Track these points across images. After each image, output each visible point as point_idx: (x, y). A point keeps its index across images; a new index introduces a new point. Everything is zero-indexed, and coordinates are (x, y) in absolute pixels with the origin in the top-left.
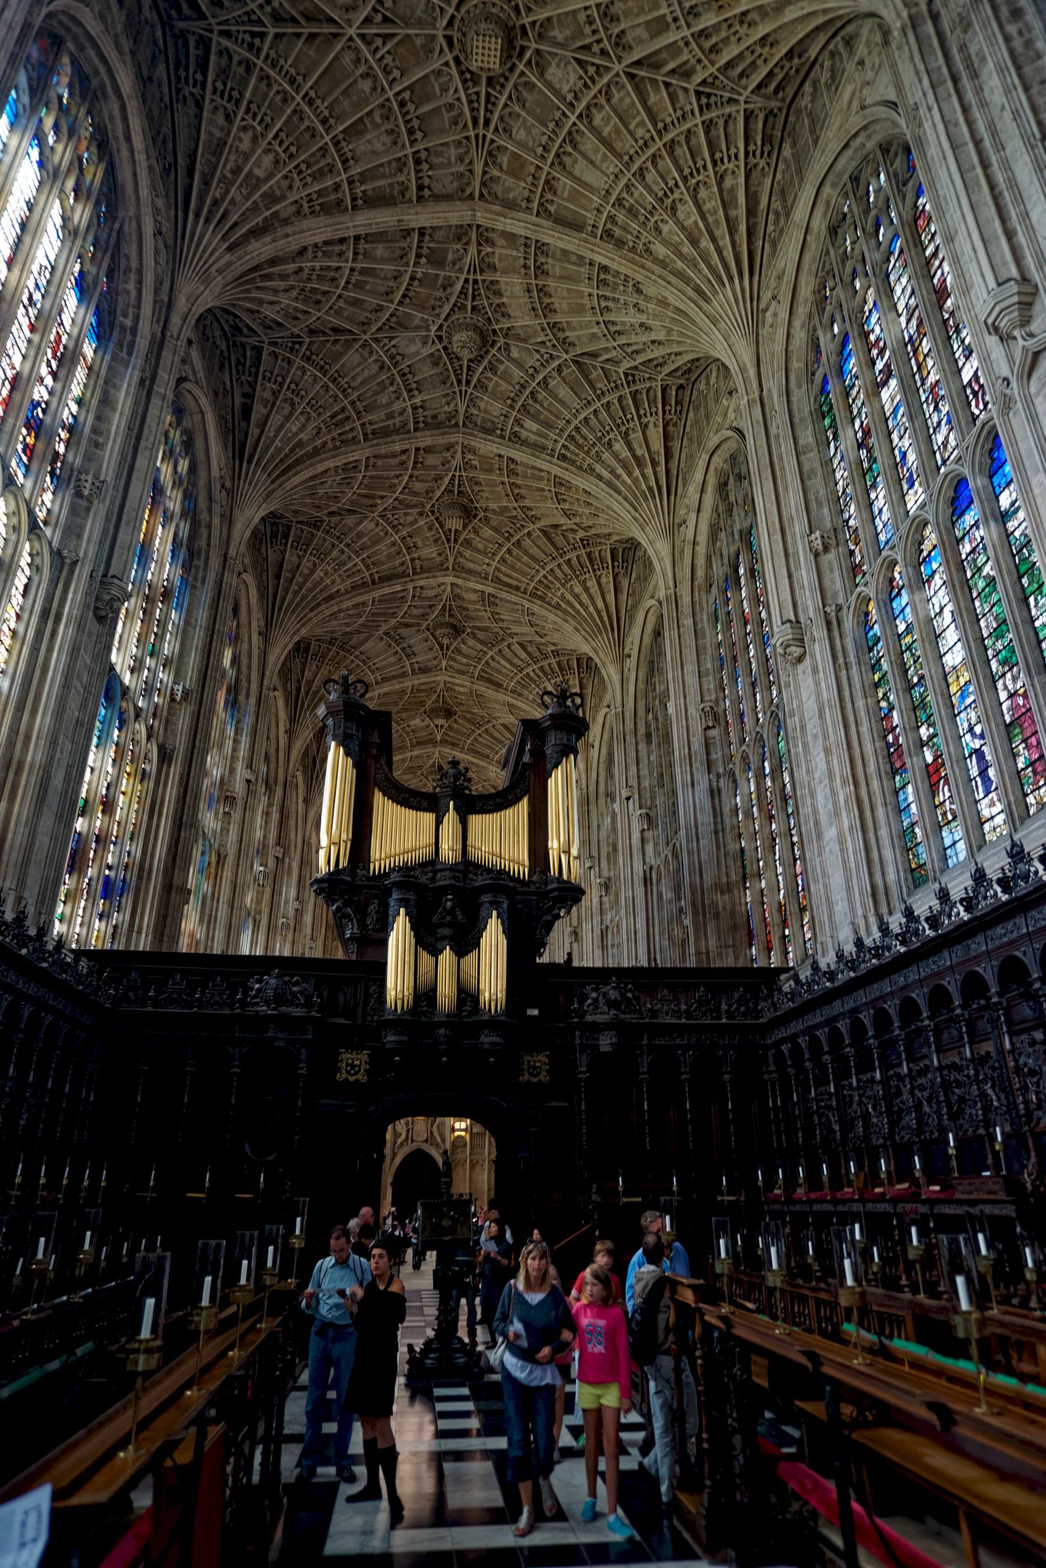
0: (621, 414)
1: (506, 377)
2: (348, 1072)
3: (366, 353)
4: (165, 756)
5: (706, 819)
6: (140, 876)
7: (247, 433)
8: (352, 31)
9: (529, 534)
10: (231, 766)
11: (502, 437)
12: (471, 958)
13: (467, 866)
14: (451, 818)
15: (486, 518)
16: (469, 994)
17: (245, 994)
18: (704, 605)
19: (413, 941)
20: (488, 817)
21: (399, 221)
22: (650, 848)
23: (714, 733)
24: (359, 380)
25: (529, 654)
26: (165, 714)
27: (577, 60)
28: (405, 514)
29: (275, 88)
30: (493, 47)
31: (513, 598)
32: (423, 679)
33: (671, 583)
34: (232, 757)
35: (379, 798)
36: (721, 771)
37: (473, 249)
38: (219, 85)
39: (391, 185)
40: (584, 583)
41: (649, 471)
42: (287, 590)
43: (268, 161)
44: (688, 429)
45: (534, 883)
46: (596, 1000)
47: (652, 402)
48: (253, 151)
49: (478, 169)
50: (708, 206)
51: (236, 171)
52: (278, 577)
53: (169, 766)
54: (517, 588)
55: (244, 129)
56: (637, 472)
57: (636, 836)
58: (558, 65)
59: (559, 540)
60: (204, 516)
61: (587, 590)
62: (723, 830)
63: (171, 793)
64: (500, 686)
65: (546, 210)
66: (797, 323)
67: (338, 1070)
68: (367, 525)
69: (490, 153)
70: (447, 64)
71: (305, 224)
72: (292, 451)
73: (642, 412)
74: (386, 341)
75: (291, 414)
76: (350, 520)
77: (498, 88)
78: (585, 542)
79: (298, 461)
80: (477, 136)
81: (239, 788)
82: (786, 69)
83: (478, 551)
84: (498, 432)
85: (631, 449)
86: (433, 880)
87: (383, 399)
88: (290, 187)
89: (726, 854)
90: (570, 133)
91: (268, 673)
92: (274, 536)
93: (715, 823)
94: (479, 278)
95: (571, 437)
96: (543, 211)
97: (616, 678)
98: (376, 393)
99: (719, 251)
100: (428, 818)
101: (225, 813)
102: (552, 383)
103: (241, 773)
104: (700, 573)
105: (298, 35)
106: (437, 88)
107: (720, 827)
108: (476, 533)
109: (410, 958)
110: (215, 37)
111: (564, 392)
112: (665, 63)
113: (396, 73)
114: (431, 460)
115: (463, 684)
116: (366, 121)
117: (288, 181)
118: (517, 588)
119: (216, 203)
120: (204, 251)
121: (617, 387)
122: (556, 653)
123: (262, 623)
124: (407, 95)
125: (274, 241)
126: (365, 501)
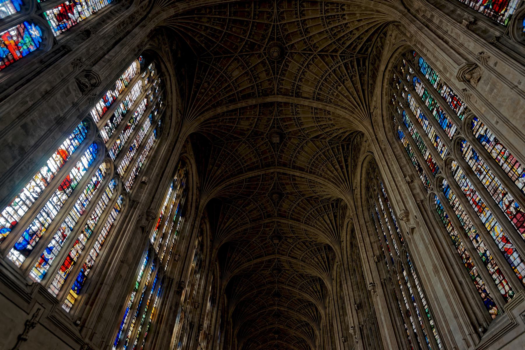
1: (285, 275)
40: (308, 310)
51: (233, 261)
66: (338, 286)
68: (257, 299)
83: (282, 301)
96: (289, 256)
97: (318, 334)
99: (323, 266)
104: (331, 321)
111: (297, 278)
115: (281, 327)
122: (305, 321)
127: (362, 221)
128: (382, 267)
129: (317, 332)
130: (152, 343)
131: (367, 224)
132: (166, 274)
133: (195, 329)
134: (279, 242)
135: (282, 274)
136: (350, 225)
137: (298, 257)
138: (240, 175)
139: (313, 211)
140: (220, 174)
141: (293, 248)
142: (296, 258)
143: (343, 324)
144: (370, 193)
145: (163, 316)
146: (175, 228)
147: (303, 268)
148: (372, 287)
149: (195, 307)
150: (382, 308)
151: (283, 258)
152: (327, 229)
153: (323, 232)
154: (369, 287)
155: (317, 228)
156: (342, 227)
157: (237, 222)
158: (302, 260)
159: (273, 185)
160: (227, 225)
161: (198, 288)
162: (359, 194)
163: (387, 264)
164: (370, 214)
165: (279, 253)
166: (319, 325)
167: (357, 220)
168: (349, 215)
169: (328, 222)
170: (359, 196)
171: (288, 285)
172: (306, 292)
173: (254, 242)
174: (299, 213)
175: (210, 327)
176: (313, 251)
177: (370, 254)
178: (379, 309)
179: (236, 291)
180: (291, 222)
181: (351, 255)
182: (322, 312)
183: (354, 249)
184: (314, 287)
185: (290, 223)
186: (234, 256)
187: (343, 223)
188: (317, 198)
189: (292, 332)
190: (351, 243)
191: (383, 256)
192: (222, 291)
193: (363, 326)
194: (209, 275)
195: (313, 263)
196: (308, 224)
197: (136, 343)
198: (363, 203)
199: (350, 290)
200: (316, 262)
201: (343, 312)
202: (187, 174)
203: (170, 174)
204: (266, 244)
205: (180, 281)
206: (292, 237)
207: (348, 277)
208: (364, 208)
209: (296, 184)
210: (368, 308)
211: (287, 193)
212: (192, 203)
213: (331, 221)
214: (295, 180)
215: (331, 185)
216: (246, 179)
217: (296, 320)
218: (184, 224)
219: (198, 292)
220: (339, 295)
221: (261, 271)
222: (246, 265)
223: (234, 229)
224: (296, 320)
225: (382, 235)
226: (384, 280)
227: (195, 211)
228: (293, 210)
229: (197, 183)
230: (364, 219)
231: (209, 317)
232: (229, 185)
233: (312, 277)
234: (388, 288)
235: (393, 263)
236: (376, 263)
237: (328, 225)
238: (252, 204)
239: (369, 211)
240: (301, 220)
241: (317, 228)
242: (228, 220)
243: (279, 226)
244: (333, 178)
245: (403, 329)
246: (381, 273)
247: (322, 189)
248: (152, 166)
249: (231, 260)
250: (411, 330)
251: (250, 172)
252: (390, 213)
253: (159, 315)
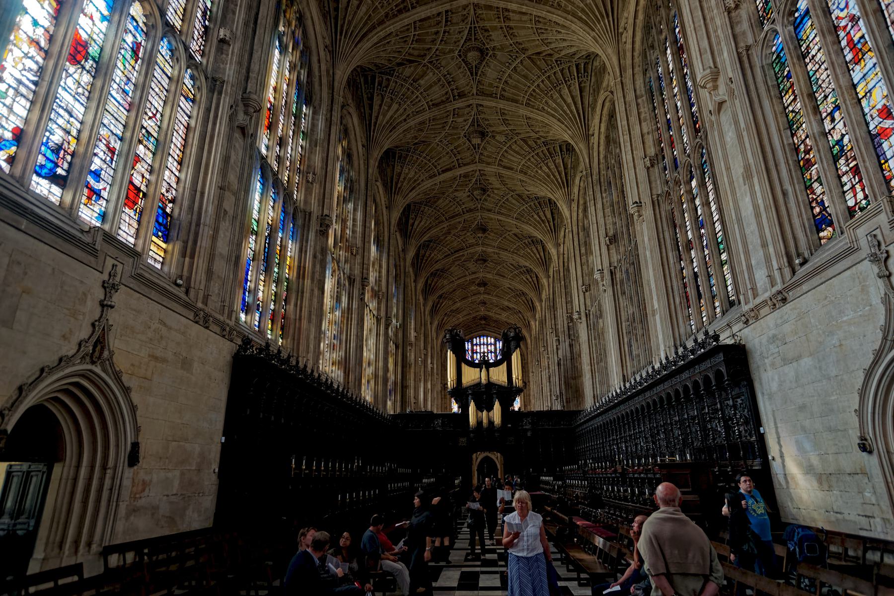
1: (493, 197)
4: (397, 347)
5: (569, 355)
12: (491, 414)
13: (490, 385)
14: (484, 370)
23: (571, 324)
25: (514, 267)
32: (474, 276)
35: (463, 365)
40: (531, 250)
41: (547, 224)
42: (421, 263)
50: (552, 167)
51: (404, 179)
52: (417, 259)
54: (507, 250)
57: (555, 347)
59: (521, 237)
60: (398, 263)
61: (532, 251)
64: (504, 277)
66: (580, 211)
71: (425, 183)
85: (540, 218)
86: (480, 389)
96: (499, 165)
97: (546, 284)
104: (566, 264)
108: (489, 234)
109: (475, 414)
111: (514, 201)
115: (489, 276)
119: (400, 188)
122: (525, 267)
127: (631, 96)
128: (657, 175)
129: (544, 281)
130: (296, 305)
131: (640, 101)
132: (298, 204)
133: (357, 284)
134: (482, 141)
135: (489, 196)
136: (607, 104)
137: (514, 165)
138: (403, 15)
139: (543, 81)
140: (366, 14)
141: (506, 151)
142: (512, 169)
143: (585, 267)
144: (651, 39)
145: (304, 268)
146: (299, 127)
147: (524, 184)
148: (636, 209)
149: (352, 254)
150: (649, 239)
151: (489, 169)
152: (567, 114)
153: (559, 120)
154: (632, 209)
155: (548, 113)
156: (594, 109)
157: (405, 109)
158: (521, 172)
159: (466, 32)
160: (388, 117)
161: (354, 225)
162: (630, 41)
163: (665, 169)
164: (647, 80)
165: (481, 161)
166: (547, 270)
167: (620, 94)
168: (608, 86)
169: (570, 100)
170: (629, 46)
171: (499, 213)
172: (527, 223)
173: (438, 145)
174: (515, 87)
175: (380, 281)
176: (541, 154)
177: (640, 153)
178: (643, 241)
179: (415, 227)
180: (502, 105)
181: (606, 157)
182: (553, 252)
183: (612, 146)
184: (541, 214)
185: (501, 106)
186: (407, 171)
187: (595, 101)
188: (550, 55)
189: (506, 283)
190: (607, 137)
191: (660, 157)
192: (392, 228)
193: (615, 268)
194: (369, 202)
195: (540, 175)
196: (533, 107)
197: (272, 307)
198: (637, 60)
199: (600, 214)
200: (545, 173)
201: (586, 250)
202: (301, 19)
203: (270, 20)
204: (459, 146)
205: (322, 216)
206: (504, 131)
207: (598, 196)
208: (637, 69)
209: (511, 28)
210: (627, 242)
211: (494, 49)
212: (320, 77)
213: (573, 98)
214: (507, 19)
215: (576, 26)
216: (415, 23)
217: (512, 265)
218: (313, 119)
219: (354, 232)
220: (580, 224)
221: (452, 192)
222: (428, 184)
223: (401, 122)
224: (512, 265)
225: (664, 120)
226: (658, 195)
227: (328, 93)
228: (506, 82)
229: (324, 38)
230: (635, 91)
231: (377, 267)
232: (385, 38)
233: (538, 198)
234: (662, 209)
235: (676, 167)
236: (648, 168)
237: (568, 106)
238: (431, 74)
239: (645, 74)
240: (521, 99)
241: (548, 113)
242: (390, 107)
243: (480, 112)
244: (583, 11)
245: (678, 268)
246: (653, 185)
247: (560, 37)
248: (232, 6)
249: (401, 179)
250: (691, 268)
251: (423, 8)
252: (684, 76)
253: (299, 267)
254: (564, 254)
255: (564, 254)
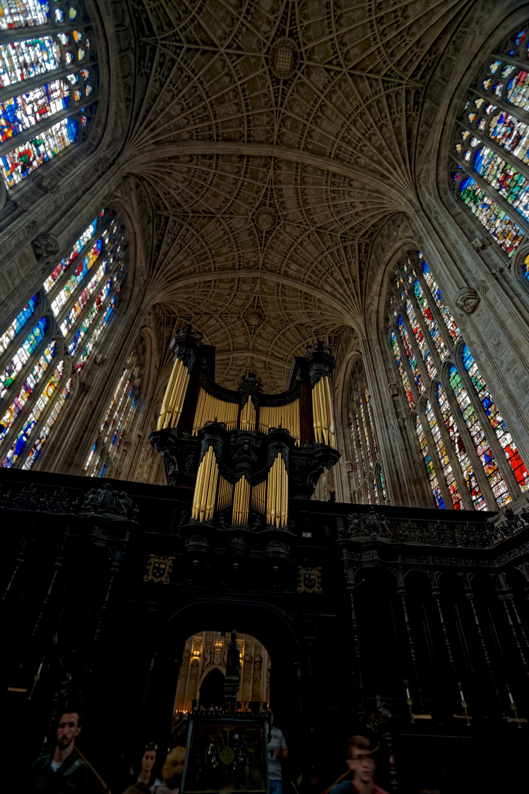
0: (338, 258)
2: (154, 574)
3: (218, 224)
5: (398, 444)
6: (51, 451)
7: (157, 258)
8: (222, 50)
9: (289, 329)
10: (131, 427)
11: (280, 274)
12: (260, 488)
15: (269, 321)
16: (258, 513)
17: (81, 502)
18: (385, 340)
19: (217, 471)
20: (273, 409)
21: (238, 149)
22: (353, 481)
24: (214, 238)
26: (89, 368)
27: (326, 69)
28: (232, 317)
29: (185, 74)
30: (287, 57)
31: (280, 364)
33: (365, 335)
34: (133, 423)
36: (405, 416)
37: (271, 171)
38: (159, 69)
39: (235, 132)
41: (352, 285)
43: (178, 108)
44: (371, 264)
45: (305, 449)
46: (358, 525)
47: (353, 252)
48: (171, 102)
49: (276, 128)
53: (86, 394)
55: (169, 91)
56: (346, 286)
58: (316, 73)
59: (304, 332)
62: (410, 448)
63: (83, 409)
65: (307, 148)
67: (146, 572)
68: (213, 322)
69: (282, 121)
70: (264, 72)
72: (179, 270)
73: (348, 256)
74: (228, 219)
75: (180, 251)
76: (205, 318)
77: (288, 86)
78: (316, 333)
79: (181, 276)
80: (277, 110)
81: (134, 438)
82: (428, 61)
84: (278, 271)
87: (224, 250)
88: (188, 124)
89: (414, 462)
90: (321, 106)
91: (158, 388)
92: (168, 323)
93: (405, 445)
94: (274, 187)
95: (313, 271)
98: (221, 247)
100: (234, 407)
101: (124, 450)
102: (305, 244)
103: (136, 431)
104: (381, 325)
105: (197, 50)
106: (260, 86)
107: (408, 447)
108: (264, 329)
110: (159, 46)
112: (368, 67)
113: (242, 75)
114: (246, 287)
116: (226, 97)
117: (187, 121)
118: (282, 359)
120: (142, 139)
121: (336, 244)
123: (158, 364)
124: (246, 86)
125: (178, 147)
126: (213, 308)
254: (378, 312)
255: (378, 312)
